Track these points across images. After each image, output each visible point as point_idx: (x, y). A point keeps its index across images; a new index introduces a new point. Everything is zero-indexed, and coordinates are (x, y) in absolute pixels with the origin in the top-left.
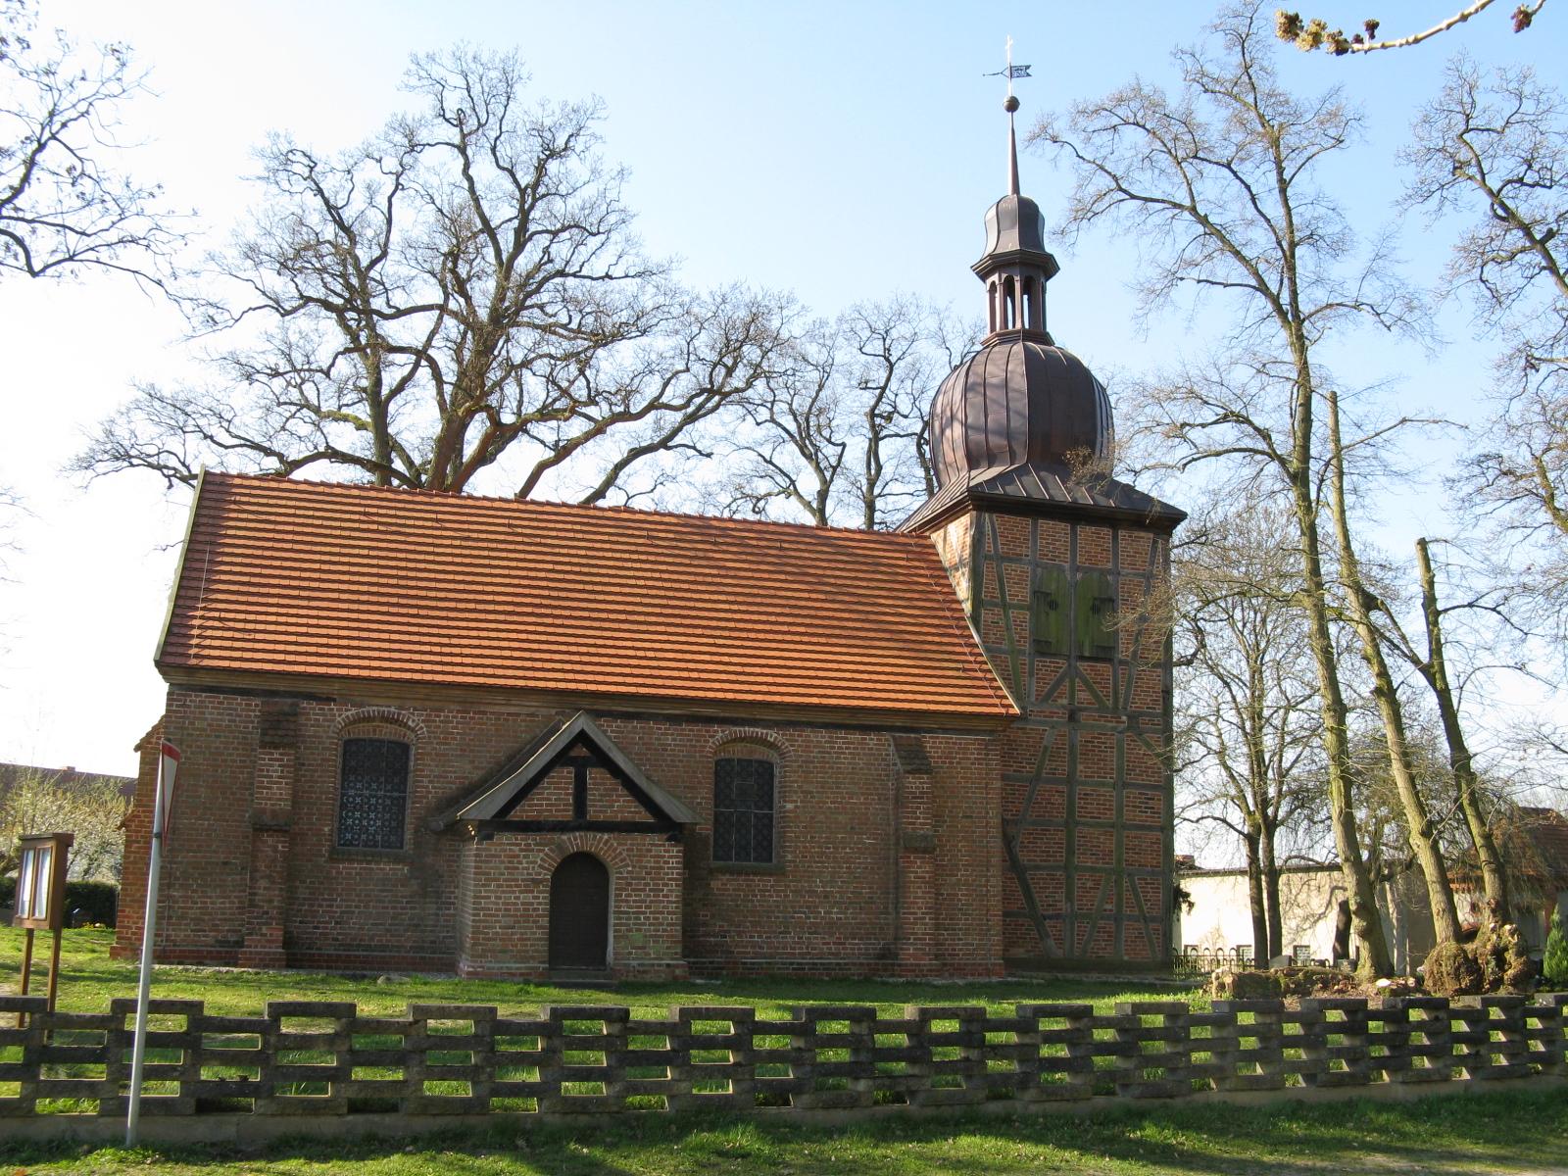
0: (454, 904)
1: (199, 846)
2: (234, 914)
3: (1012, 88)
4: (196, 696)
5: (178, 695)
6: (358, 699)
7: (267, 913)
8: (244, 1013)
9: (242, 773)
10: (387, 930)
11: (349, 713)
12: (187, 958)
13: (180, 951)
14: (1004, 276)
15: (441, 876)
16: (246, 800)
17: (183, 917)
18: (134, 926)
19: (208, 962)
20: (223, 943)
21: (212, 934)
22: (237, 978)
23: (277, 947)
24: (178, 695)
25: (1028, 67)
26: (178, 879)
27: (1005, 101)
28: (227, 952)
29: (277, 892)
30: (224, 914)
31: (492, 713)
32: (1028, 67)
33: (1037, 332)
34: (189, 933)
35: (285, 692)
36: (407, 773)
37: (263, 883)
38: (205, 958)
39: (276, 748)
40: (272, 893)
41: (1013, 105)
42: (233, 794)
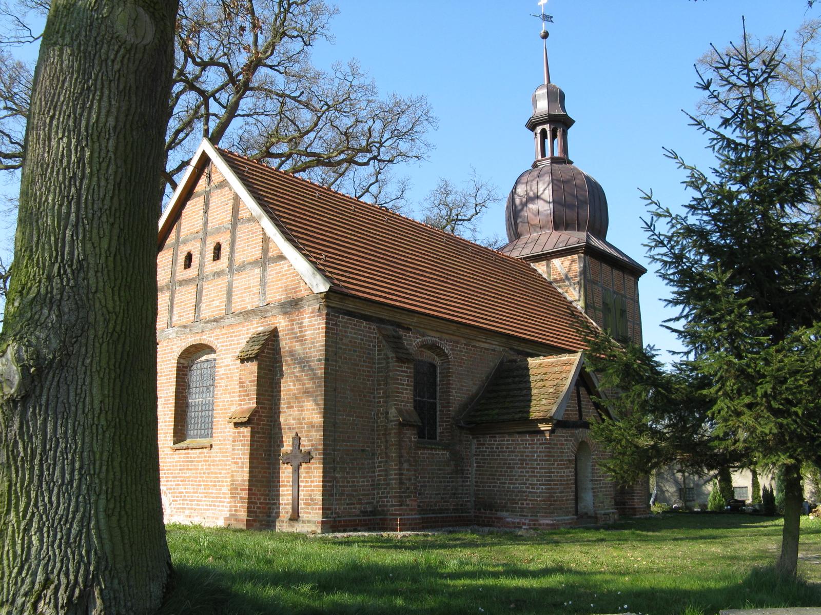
0: (469, 478)
1: (349, 437)
2: (369, 490)
3: (544, 27)
4: (342, 318)
5: (333, 316)
6: (422, 330)
7: (408, 488)
8: (258, 561)
9: (368, 380)
10: (442, 498)
11: (418, 340)
12: (348, 526)
13: (344, 521)
14: (552, 127)
15: (463, 459)
16: (371, 401)
17: (342, 494)
18: (258, 502)
19: (359, 528)
20: (364, 513)
21: (358, 506)
22: (602, 540)
23: (415, 514)
24: (333, 316)
25: (552, 17)
26: (338, 463)
27: (542, 32)
28: (370, 520)
29: (413, 472)
30: (364, 490)
31: (479, 347)
32: (552, 17)
33: (564, 160)
34: (346, 506)
35: (388, 321)
36: (436, 386)
37: (406, 466)
38: (357, 525)
39: (404, 363)
40: (410, 473)
41: (546, 36)
42: (365, 396)
